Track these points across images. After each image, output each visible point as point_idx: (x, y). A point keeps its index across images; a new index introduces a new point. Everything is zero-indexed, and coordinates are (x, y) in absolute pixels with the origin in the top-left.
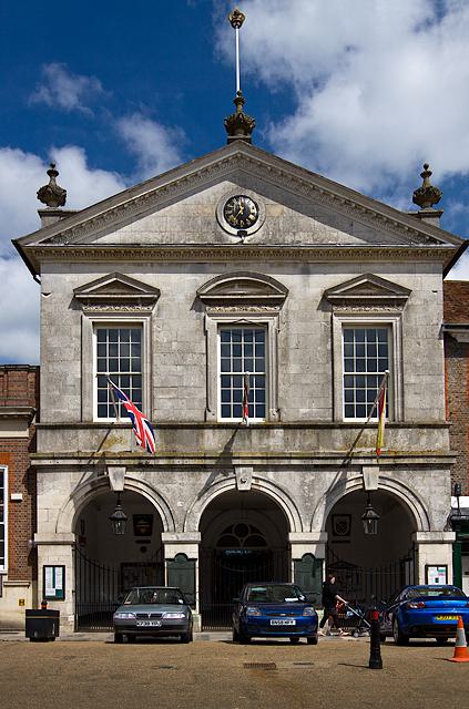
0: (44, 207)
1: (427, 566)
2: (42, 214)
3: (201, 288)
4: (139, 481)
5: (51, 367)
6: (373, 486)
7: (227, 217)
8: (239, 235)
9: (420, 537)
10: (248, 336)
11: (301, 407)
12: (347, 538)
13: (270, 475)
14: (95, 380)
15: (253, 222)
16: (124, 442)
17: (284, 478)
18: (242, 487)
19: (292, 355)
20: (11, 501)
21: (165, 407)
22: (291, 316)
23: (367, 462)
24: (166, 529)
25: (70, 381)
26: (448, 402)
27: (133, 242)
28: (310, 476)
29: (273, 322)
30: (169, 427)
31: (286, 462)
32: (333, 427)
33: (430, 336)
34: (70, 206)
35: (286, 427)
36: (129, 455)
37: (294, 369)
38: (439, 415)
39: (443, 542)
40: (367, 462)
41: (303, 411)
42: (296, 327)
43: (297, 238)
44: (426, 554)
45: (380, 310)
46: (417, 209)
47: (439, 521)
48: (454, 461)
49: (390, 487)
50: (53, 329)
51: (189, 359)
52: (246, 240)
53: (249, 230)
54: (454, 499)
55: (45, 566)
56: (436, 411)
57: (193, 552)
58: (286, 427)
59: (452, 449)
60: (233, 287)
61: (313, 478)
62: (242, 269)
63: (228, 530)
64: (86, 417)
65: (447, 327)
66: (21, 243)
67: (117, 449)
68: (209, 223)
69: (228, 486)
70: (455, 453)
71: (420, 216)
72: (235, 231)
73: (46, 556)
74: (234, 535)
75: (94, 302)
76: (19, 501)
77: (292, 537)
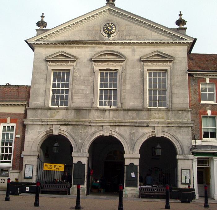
0: (38, 28)
1: (182, 170)
2: (37, 30)
3: (93, 56)
4: (65, 131)
6: (159, 135)
7: (104, 30)
8: (108, 36)
9: (178, 157)
10: (111, 74)
11: (131, 102)
13: (117, 129)
14: (51, 92)
15: (114, 32)
16: (61, 115)
17: (122, 130)
18: (105, 134)
19: (127, 82)
20: (15, 138)
21: (78, 101)
24: (74, 151)
26: (190, 101)
27: (69, 40)
28: (134, 130)
30: (78, 110)
31: (123, 124)
32: (142, 110)
35: (124, 110)
37: (128, 87)
38: (186, 105)
39: (188, 159)
42: (129, 71)
44: (181, 165)
46: (177, 27)
47: (186, 150)
48: (192, 125)
52: (111, 39)
53: (112, 35)
54: (193, 141)
55: (25, 165)
57: (84, 161)
58: (124, 110)
60: (105, 56)
61: (134, 131)
62: (109, 49)
64: (46, 105)
68: (97, 33)
69: (100, 134)
71: (177, 29)
72: (107, 35)
73: (26, 161)
75: (53, 61)
77: (125, 156)
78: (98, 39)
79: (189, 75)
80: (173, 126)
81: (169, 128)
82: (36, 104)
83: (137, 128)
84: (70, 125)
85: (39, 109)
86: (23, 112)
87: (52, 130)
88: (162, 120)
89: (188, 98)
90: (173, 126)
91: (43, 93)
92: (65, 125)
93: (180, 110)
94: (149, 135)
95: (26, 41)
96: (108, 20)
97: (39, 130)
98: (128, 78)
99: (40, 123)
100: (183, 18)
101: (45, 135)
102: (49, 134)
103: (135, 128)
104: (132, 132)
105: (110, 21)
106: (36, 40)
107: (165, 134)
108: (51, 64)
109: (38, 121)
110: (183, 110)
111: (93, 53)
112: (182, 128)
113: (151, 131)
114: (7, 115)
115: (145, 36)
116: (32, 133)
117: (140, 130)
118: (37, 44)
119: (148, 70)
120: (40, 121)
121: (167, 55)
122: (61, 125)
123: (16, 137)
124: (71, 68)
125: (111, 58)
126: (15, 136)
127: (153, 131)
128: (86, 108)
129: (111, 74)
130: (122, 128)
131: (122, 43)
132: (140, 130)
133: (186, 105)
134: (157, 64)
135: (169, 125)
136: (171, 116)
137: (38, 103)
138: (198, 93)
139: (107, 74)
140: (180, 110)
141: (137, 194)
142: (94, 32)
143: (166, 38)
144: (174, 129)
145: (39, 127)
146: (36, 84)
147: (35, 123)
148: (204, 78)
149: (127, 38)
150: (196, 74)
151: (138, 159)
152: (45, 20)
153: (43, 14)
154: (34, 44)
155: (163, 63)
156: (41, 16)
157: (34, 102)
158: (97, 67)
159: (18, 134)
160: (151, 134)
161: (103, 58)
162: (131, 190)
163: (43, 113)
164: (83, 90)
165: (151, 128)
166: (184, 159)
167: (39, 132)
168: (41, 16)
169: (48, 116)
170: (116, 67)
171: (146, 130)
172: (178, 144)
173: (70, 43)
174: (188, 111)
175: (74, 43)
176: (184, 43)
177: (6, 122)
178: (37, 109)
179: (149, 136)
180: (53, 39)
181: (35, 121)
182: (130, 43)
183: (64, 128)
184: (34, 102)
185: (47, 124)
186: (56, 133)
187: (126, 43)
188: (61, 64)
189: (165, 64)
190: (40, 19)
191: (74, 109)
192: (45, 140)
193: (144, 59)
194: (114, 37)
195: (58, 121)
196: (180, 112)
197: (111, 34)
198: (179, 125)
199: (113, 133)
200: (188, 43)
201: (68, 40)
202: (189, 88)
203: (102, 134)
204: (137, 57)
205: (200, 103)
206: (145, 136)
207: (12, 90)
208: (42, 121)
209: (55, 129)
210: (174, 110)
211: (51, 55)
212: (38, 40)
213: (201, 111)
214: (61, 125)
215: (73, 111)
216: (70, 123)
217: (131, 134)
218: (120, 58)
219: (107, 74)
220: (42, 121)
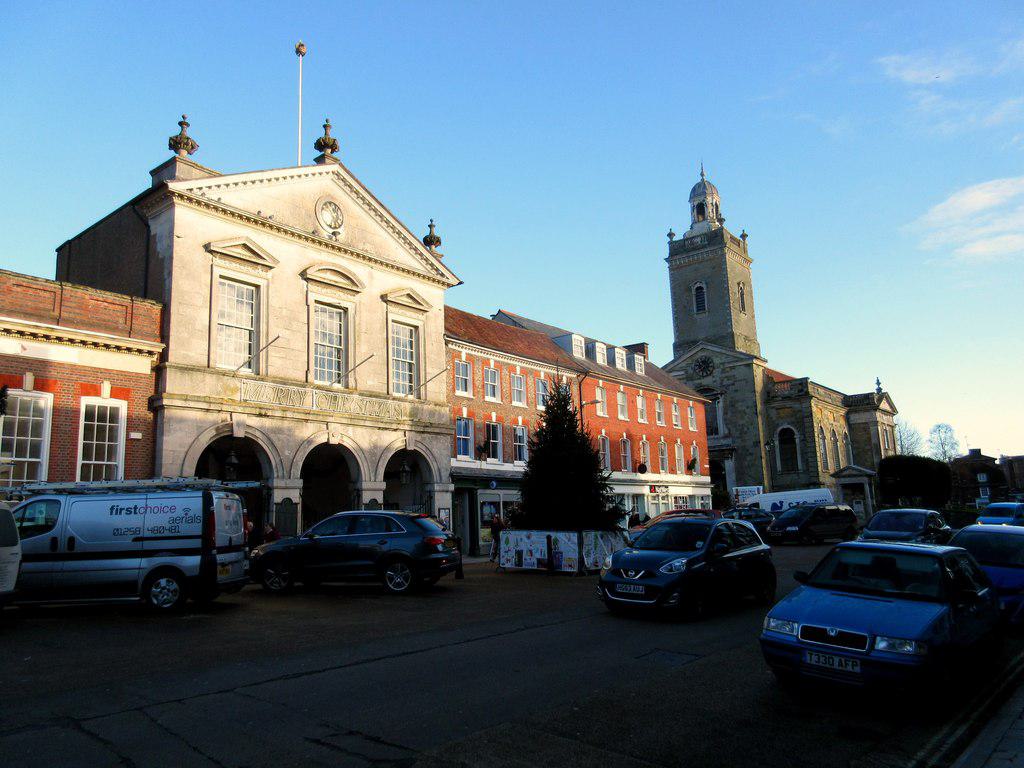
20: (129, 440)
39: (447, 491)
41: (370, 383)
47: (445, 475)
49: (420, 449)
50: (184, 273)
57: (296, 496)
76: (138, 440)
82: (188, 356)
99: (205, 406)
100: (437, 232)
114: (100, 375)
116: (180, 429)
120: (204, 402)
126: (128, 435)
130: (359, 429)
137: (192, 354)
143: (420, 267)
147: (192, 404)
154: (181, 196)
156: (181, 124)
157: (182, 352)
166: (443, 491)
172: (435, 464)
184: (182, 352)
199: (345, 439)
211: (223, 240)
212: (191, 190)
216: (269, 413)
218: (352, 286)
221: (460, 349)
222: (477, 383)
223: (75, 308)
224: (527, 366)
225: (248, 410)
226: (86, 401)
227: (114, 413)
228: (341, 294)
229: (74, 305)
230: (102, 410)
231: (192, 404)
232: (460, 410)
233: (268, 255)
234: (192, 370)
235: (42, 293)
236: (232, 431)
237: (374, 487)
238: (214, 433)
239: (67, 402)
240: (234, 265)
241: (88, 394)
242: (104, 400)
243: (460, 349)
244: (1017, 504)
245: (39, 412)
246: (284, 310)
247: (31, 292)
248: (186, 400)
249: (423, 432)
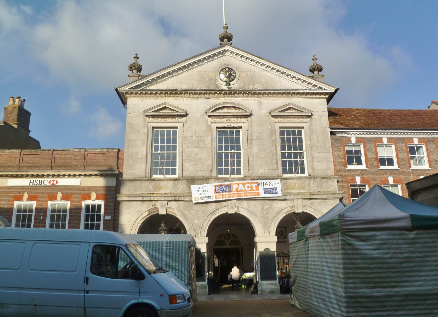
0: (131, 73)
2: (129, 76)
5: (130, 149)
8: (226, 85)
10: (232, 133)
12: (284, 240)
15: (233, 80)
18: (230, 212)
19: (254, 142)
22: (253, 123)
23: (296, 197)
25: (140, 156)
26: (335, 166)
27: (174, 88)
29: (244, 126)
33: (323, 133)
34: (142, 73)
36: (169, 195)
37: (256, 149)
40: (296, 197)
41: (261, 171)
43: (255, 87)
45: (297, 120)
51: (201, 144)
53: (231, 83)
56: (330, 171)
59: (339, 190)
61: (267, 206)
63: (221, 236)
65: (331, 129)
66: (119, 89)
67: (163, 191)
69: (222, 211)
70: (341, 192)
74: (223, 239)
76: (109, 220)
78: (212, 87)
79: (332, 133)
80: (316, 199)
81: (311, 201)
83: (271, 202)
84: (182, 201)
85: (138, 180)
86: (114, 184)
87: (157, 209)
88: (302, 191)
89: (333, 163)
90: (316, 199)
91: (142, 159)
92: (175, 200)
93: (324, 178)
94: (286, 210)
95: (117, 90)
96: (225, 64)
97: (139, 209)
98: (255, 138)
99: (140, 199)
101: (148, 215)
102: (153, 214)
103: (268, 202)
104: (265, 208)
105: (227, 65)
106: (130, 88)
107: (308, 208)
108: (152, 119)
109: (137, 196)
110: (327, 178)
111: (208, 107)
112: (328, 200)
113: (289, 206)
114: (91, 189)
115: (273, 85)
117: (276, 205)
118: (132, 93)
119: (280, 128)
120: (139, 196)
121: (303, 108)
122: (169, 201)
123: (106, 219)
124: (180, 125)
125: (232, 113)
126: (104, 218)
127: (292, 205)
128: (202, 177)
129: (232, 133)
131: (245, 93)
132: (276, 205)
133: (331, 172)
134: (291, 120)
135: (312, 197)
136: (313, 186)
137: (135, 172)
138: (343, 156)
139: (226, 133)
140: (324, 178)
141: (276, 289)
142: (207, 79)
144: (318, 203)
145: (139, 204)
146: (131, 146)
147: (133, 199)
148: (349, 137)
149: (251, 87)
150: (339, 132)
151: (275, 243)
152: (139, 62)
153: (137, 55)
154: (127, 93)
155: (298, 118)
156: (134, 58)
157: (130, 171)
158: (214, 124)
159: (108, 215)
160: (289, 209)
161: (221, 112)
162: (272, 284)
163: (144, 185)
164: (197, 154)
165: (289, 202)
167: (138, 211)
168: (134, 58)
169: (150, 189)
170: (239, 124)
171: (283, 204)
173: (176, 93)
174: (334, 178)
175: (181, 93)
176: (322, 94)
177: (89, 198)
178: (134, 180)
179: (286, 212)
180: (153, 87)
181: (133, 197)
182: (255, 93)
183: (173, 205)
184: (130, 171)
185: (150, 201)
186: (162, 212)
187: (250, 93)
188: (165, 119)
189: (301, 119)
190: (133, 61)
191: (186, 180)
192: (118, 221)
193: (275, 114)
194: (235, 85)
195: (166, 195)
196: (324, 180)
197: (230, 81)
198: (324, 196)
199: (240, 209)
200: (327, 93)
201: (173, 88)
202: (332, 150)
203: (225, 212)
204: (265, 111)
205: (347, 168)
206: (281, 213)
207: (97, 155)
208: (143, 197)
209: (162, 207)
210: (316, 178)
213: (349, 178)
214: (169, 201)
215: (185, 182)
216: (182, 198)
217: (262, 209)
219: (226, 133)
220: (143, 197)
221: (349, 135)
222: (370, 157)
223: (80, 159)
224: (423, 136)
225: (166, 199)
226: (84, 203)
227: (99, 207)
228: (235, 119)
229: (80, 158)
230: (93, 206)
231: (133, 199)
232: (354, 179)
233: (179, 109)
234: (134, 180)
235: (67, 156)
236: (158, 211)
237: (266, 240)
238: (147, 213)
239: (77, 204)
240: (160, 119)
241: (85, 199)
242: (93, 201)
243: (349, 135)
244: (223, 287)
245: (31, 211)
246: (194, 138)
247: (63, 156)
248: (129, 197)
249: (311, 199)
